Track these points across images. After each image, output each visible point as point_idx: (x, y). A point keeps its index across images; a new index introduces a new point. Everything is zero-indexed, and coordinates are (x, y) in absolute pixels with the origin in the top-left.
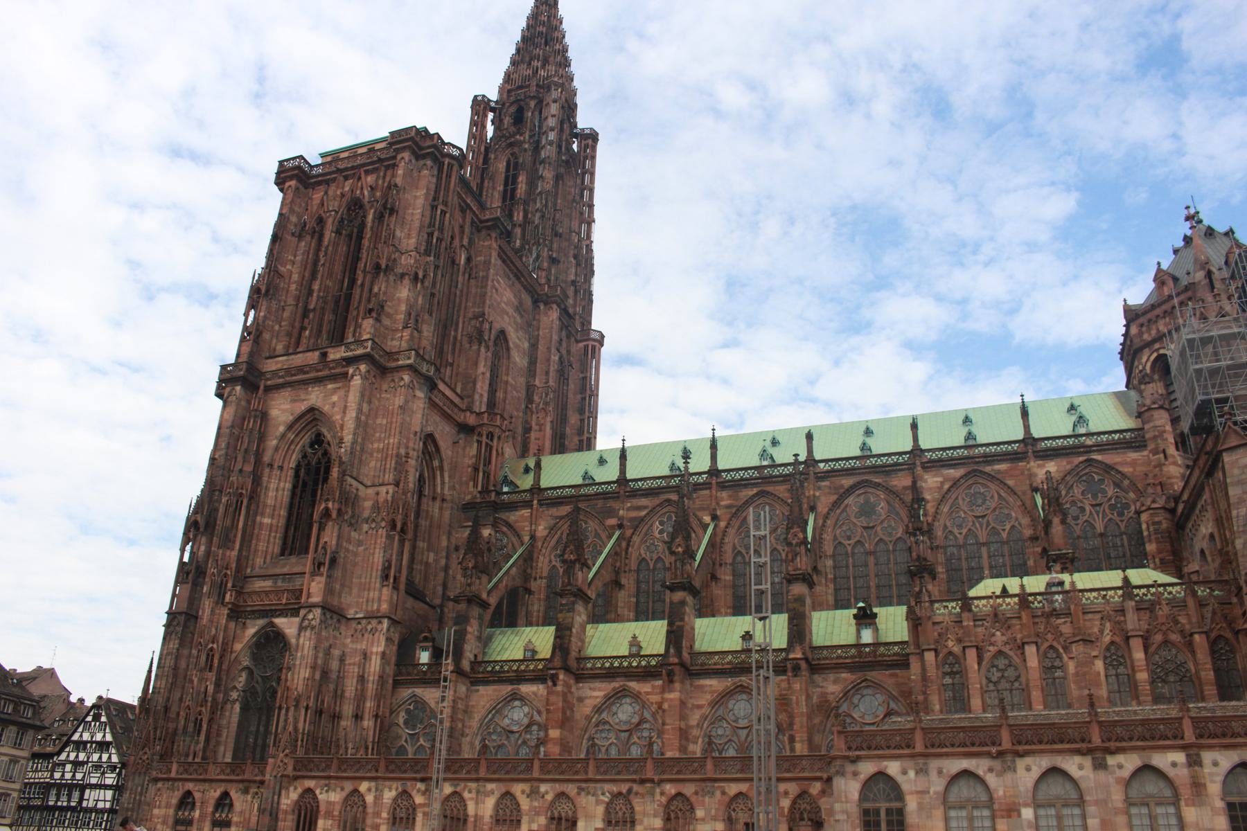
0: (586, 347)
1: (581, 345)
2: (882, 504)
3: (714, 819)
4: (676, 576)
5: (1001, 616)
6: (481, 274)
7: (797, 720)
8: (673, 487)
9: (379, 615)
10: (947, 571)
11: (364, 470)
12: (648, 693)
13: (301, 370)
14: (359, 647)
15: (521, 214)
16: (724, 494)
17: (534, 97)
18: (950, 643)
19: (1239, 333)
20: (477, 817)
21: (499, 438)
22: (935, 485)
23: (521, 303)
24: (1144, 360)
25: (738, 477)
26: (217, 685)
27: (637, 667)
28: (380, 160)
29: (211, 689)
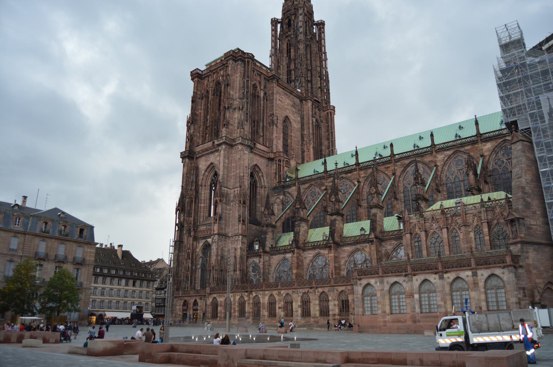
0: (328, 113)
1: (326, 112)
3: (334, 300)
5: (434, 218)
7: (373, 261)
11: (229, 183)
12: (327, 254)
13: (207, 150)
15: (293, 65)
16: (362, 172)
17: (293, 14)
20: (264, 304)
21: (283, 160)
22: (441, 159)
23: (294, 103)
26: (192, 263)
27: (322, 245)
28: (224, 65)
29: (190, 265)
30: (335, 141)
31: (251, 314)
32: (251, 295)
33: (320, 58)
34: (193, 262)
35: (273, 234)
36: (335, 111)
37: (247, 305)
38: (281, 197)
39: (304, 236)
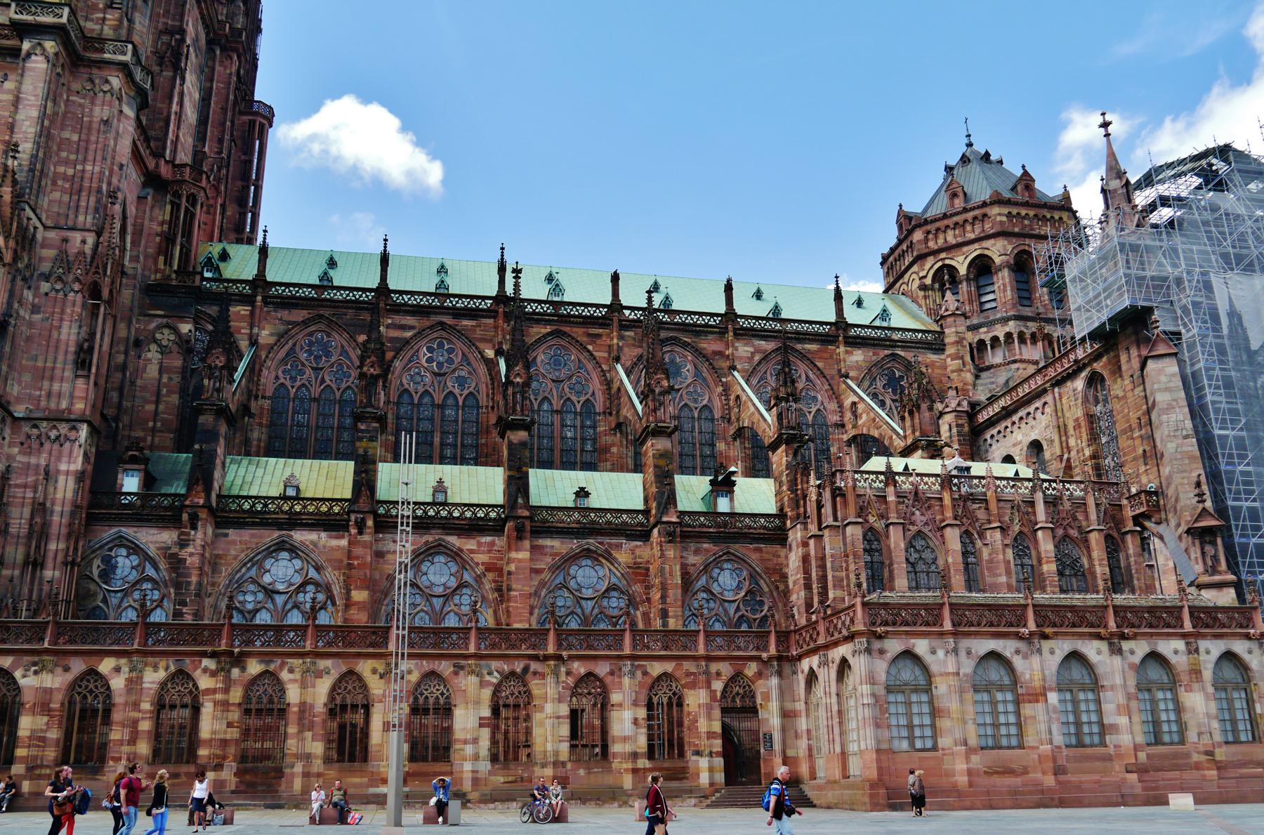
0: (252, 124)
1: (246, 118)
2: (689, 367)
3: (635, 704)
4: (514, 410)
8: (448, 308)
9: (72, 417)
10: (753, 447)
12: (472, 551)
14: (33, 460)
18: (871, 519)
19: (1161, 247)
20: (304, 707)
21: (202, 204)
24: (928, 266)
27: (458, 518)
31: (232, 750)
37: (207, 710)
38: (185, 328)
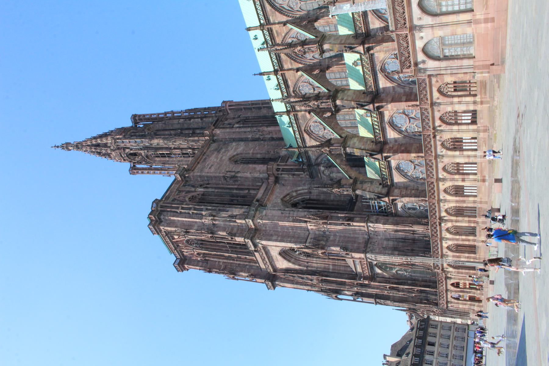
0: (230, 109)
1: (229, 112)
6: (206, 179)
8: (286, 90)
11: (302, 235)
12: (390, 113)
16: (286, 67)
20: (457, 202)
21: (278, 165)
23: (216, 150)
25: (276, 61)
28: (167, 235)
30: (262, 101)
32: (445, 218)
33: (170, 119)
34: (402, 283)
35: (366, 182)
36: (229, 101)
38: (322, 168)
39: (367, 142)
